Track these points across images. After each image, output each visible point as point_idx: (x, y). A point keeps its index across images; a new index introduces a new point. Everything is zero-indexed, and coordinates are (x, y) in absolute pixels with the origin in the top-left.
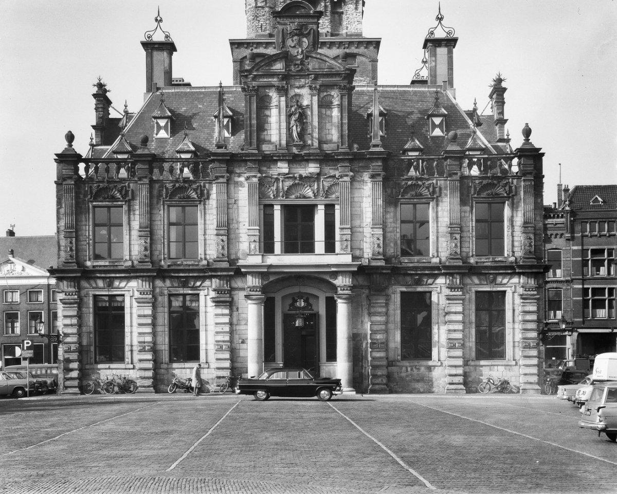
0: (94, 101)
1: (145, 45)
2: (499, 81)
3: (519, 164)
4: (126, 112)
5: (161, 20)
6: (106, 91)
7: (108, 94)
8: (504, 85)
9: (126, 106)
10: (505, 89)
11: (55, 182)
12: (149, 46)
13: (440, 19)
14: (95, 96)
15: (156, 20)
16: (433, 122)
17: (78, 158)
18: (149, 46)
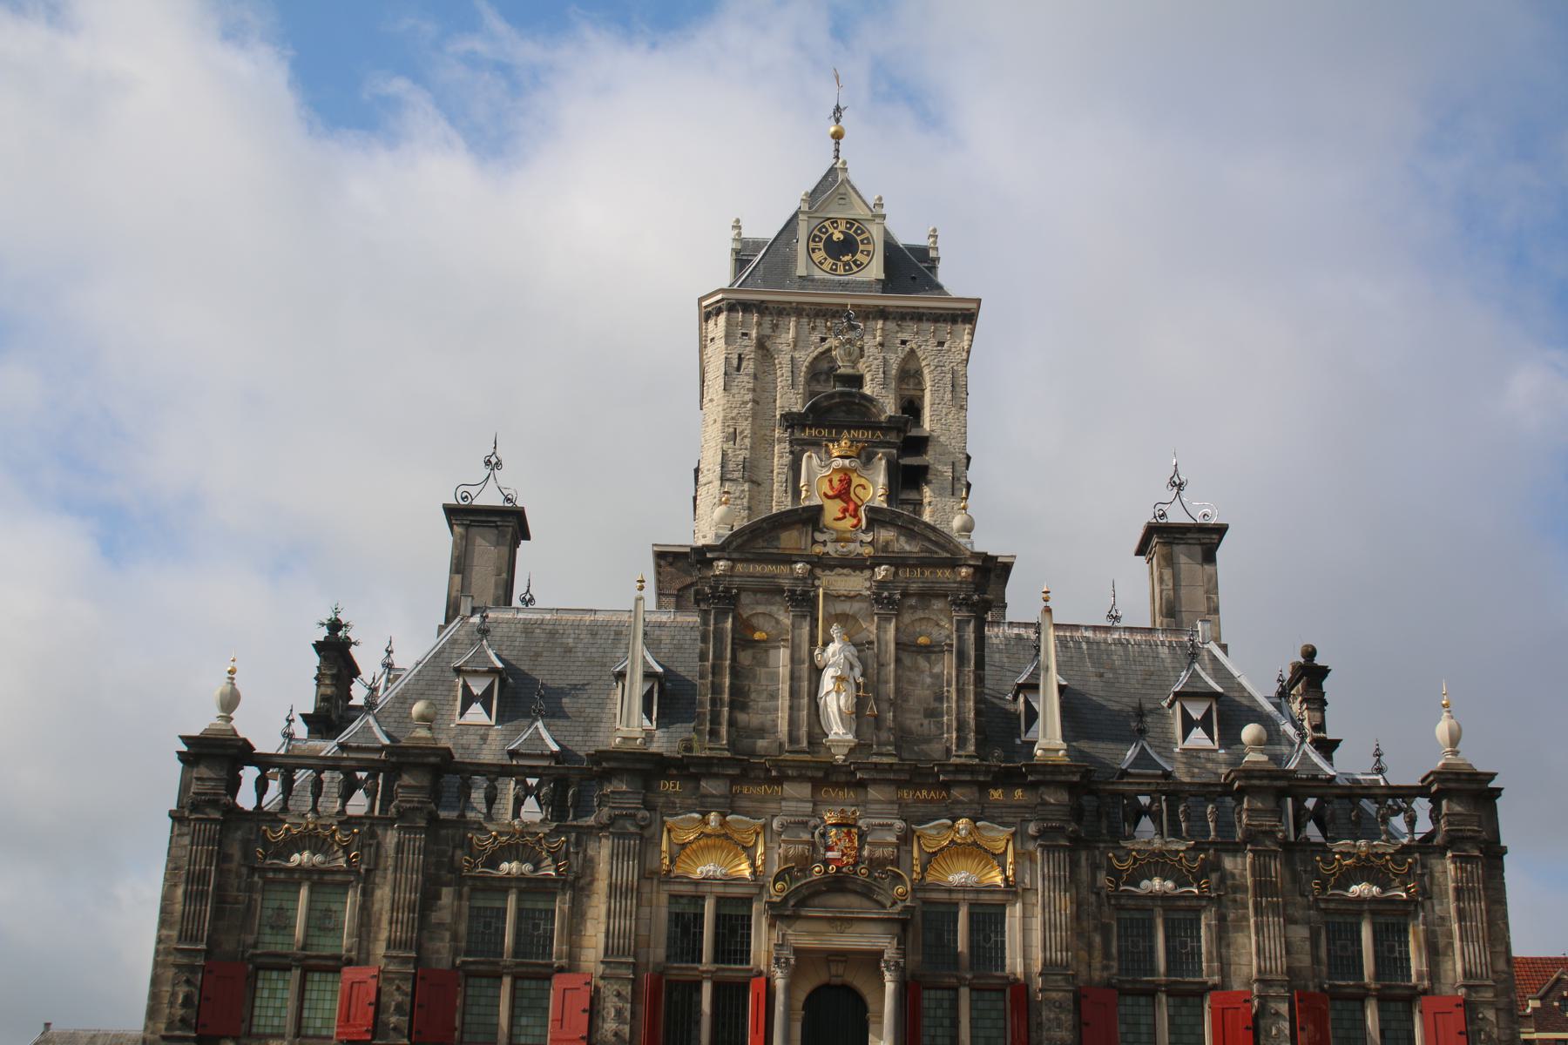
0: (316, 660)
1: (452, 512)
2: (1310, 653)
3: (1435, 816)
4: (389, 666)
5: (498, 464)
6: (347, 643)
7: (353, 650)
8: (1319, 661)
9: (389, 652)
10: (1324, 672)
11: (172, 814)
12: (461, 515)
13: (1180, 486)
14: (319, 647)
15: (488, 463)
16: (1185, 715)
17: (242, 752)
18: (461, 515)
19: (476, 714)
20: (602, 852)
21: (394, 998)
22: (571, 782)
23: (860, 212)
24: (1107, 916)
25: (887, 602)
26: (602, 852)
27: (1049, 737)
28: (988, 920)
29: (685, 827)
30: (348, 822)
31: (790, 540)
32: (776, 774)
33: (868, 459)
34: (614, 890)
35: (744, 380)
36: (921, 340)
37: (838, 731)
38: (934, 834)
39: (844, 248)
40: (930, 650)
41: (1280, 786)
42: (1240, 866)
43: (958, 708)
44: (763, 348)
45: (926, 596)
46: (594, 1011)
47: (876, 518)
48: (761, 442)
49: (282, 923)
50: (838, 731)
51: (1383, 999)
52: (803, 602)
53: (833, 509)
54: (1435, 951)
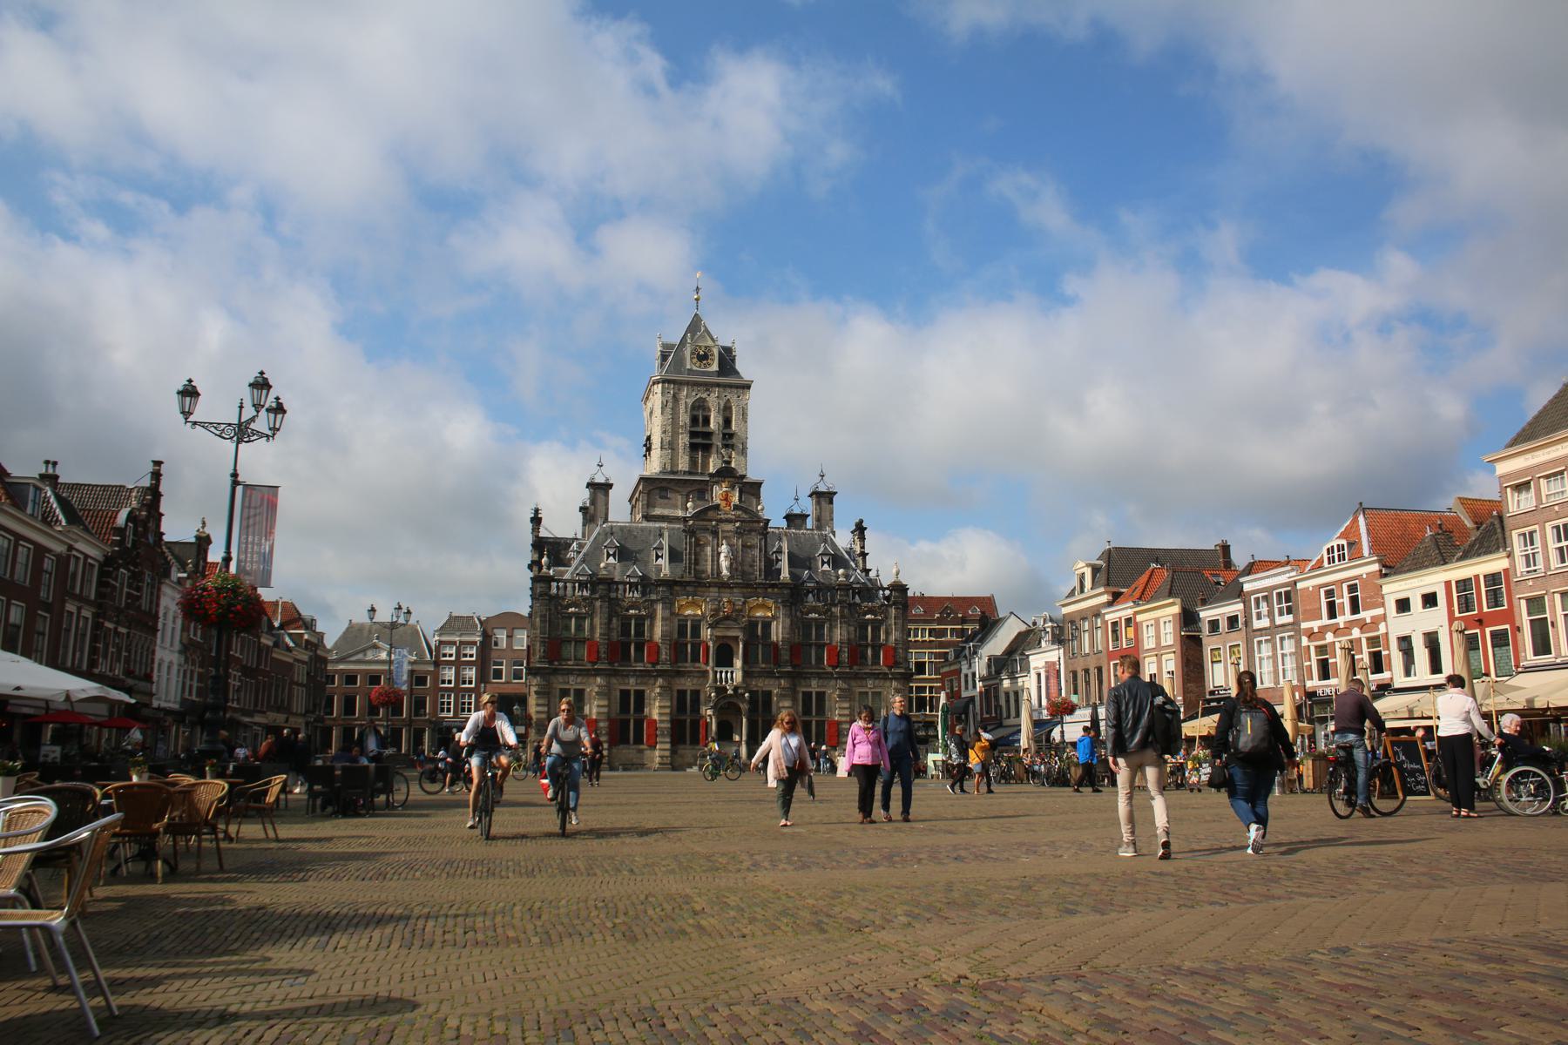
19: (611, 560)
20: (659, 607)
21: (602, 649)
22: (645, 584)
23: (710, 343)
24: (800, 625)
25: (739, 533)
26: (659, 607)
27: (785, 574)
28: (767, 625)
29: (683, 600)
30: (585, 599)
31: (711, 514)
32: (711, 585)
33: (733, 488)
34: (663, 619)
35: (668, 410)
36: (732, 396)
37: (725, 572)
38: (753, 601)
39: (704, 357)
40: (751, 547)
41: (846, 588)
42: (837, 610)
43: (759, 565)
44: (675, 398)
45: (750, 531)
46: (658, 653)
47: (736, 507)
48: (675, 434)
49: (568, 628)
50: (725, 572)
51: (873, 648)
52: (715, 533)
53: (723, 504)
54: (888, 633)
